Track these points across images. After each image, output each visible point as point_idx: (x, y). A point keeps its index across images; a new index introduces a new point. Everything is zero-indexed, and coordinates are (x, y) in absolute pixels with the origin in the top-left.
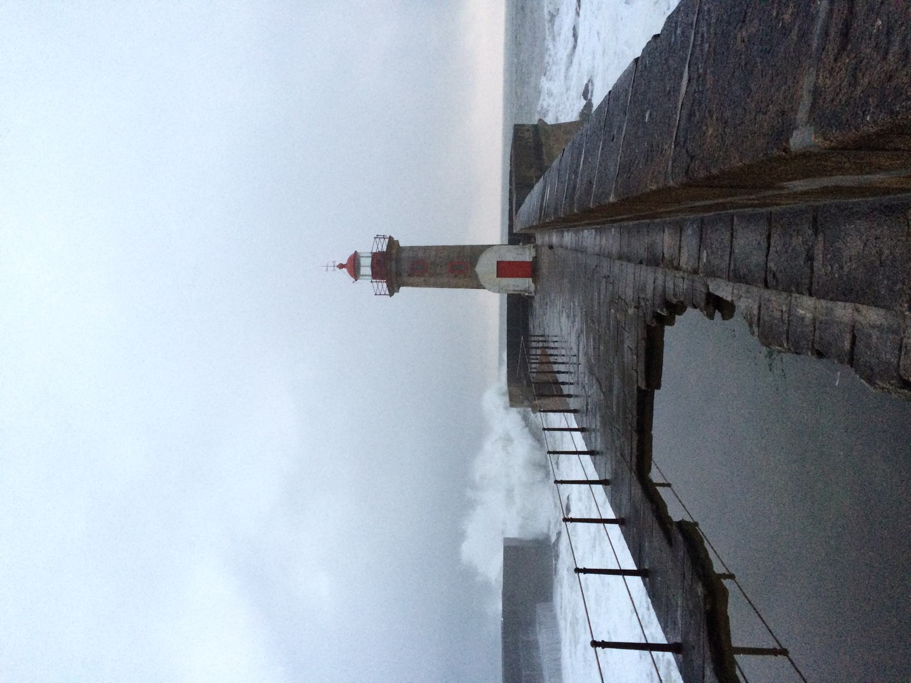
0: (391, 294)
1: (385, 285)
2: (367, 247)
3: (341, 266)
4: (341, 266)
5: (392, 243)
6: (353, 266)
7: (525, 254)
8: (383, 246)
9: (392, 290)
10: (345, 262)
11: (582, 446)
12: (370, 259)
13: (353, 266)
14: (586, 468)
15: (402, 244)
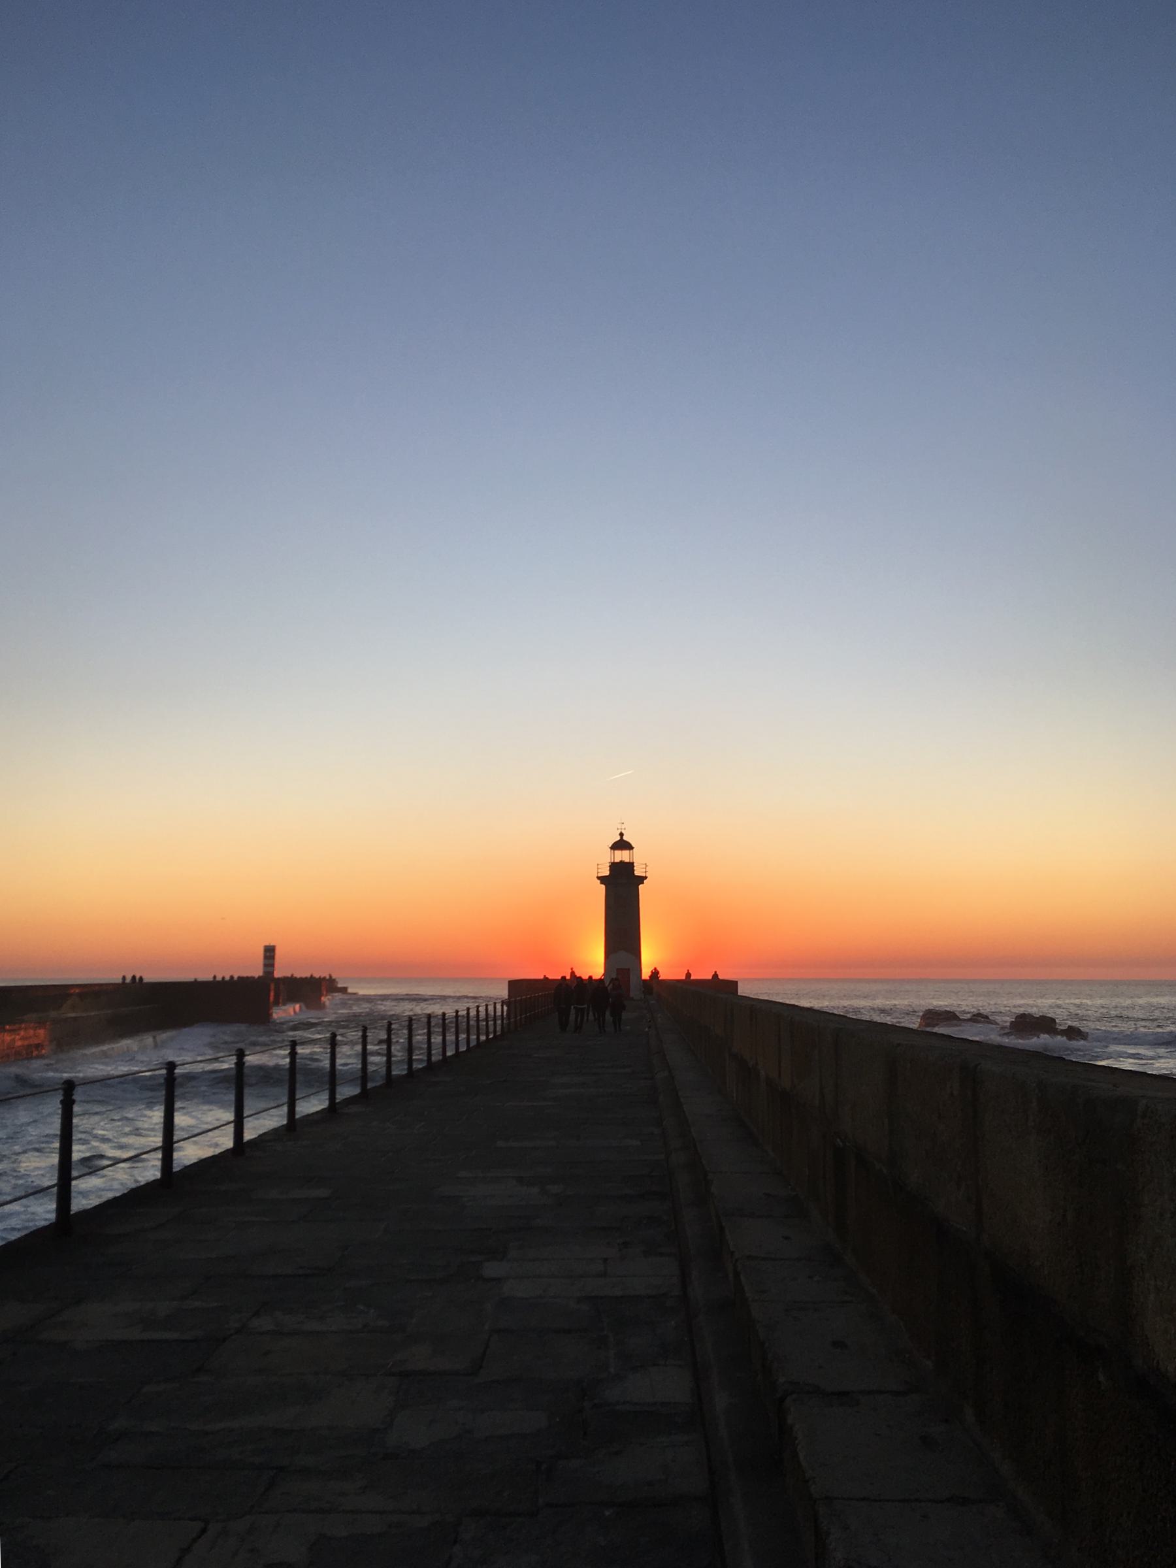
0: (598, 878)
1: (607, 873)
2: (640, 860)
3: (621, 835)
4: (621, 835)
5: (642, 879)
6: (622, 844)
7: (635, 993)
8: (638, 872)
9: (602, 879)
10: (625, 838)
11: (416, 1066)
12: (627, 860)
13: (622, 844)
14: (398, 1071)
15: (641, 886)
